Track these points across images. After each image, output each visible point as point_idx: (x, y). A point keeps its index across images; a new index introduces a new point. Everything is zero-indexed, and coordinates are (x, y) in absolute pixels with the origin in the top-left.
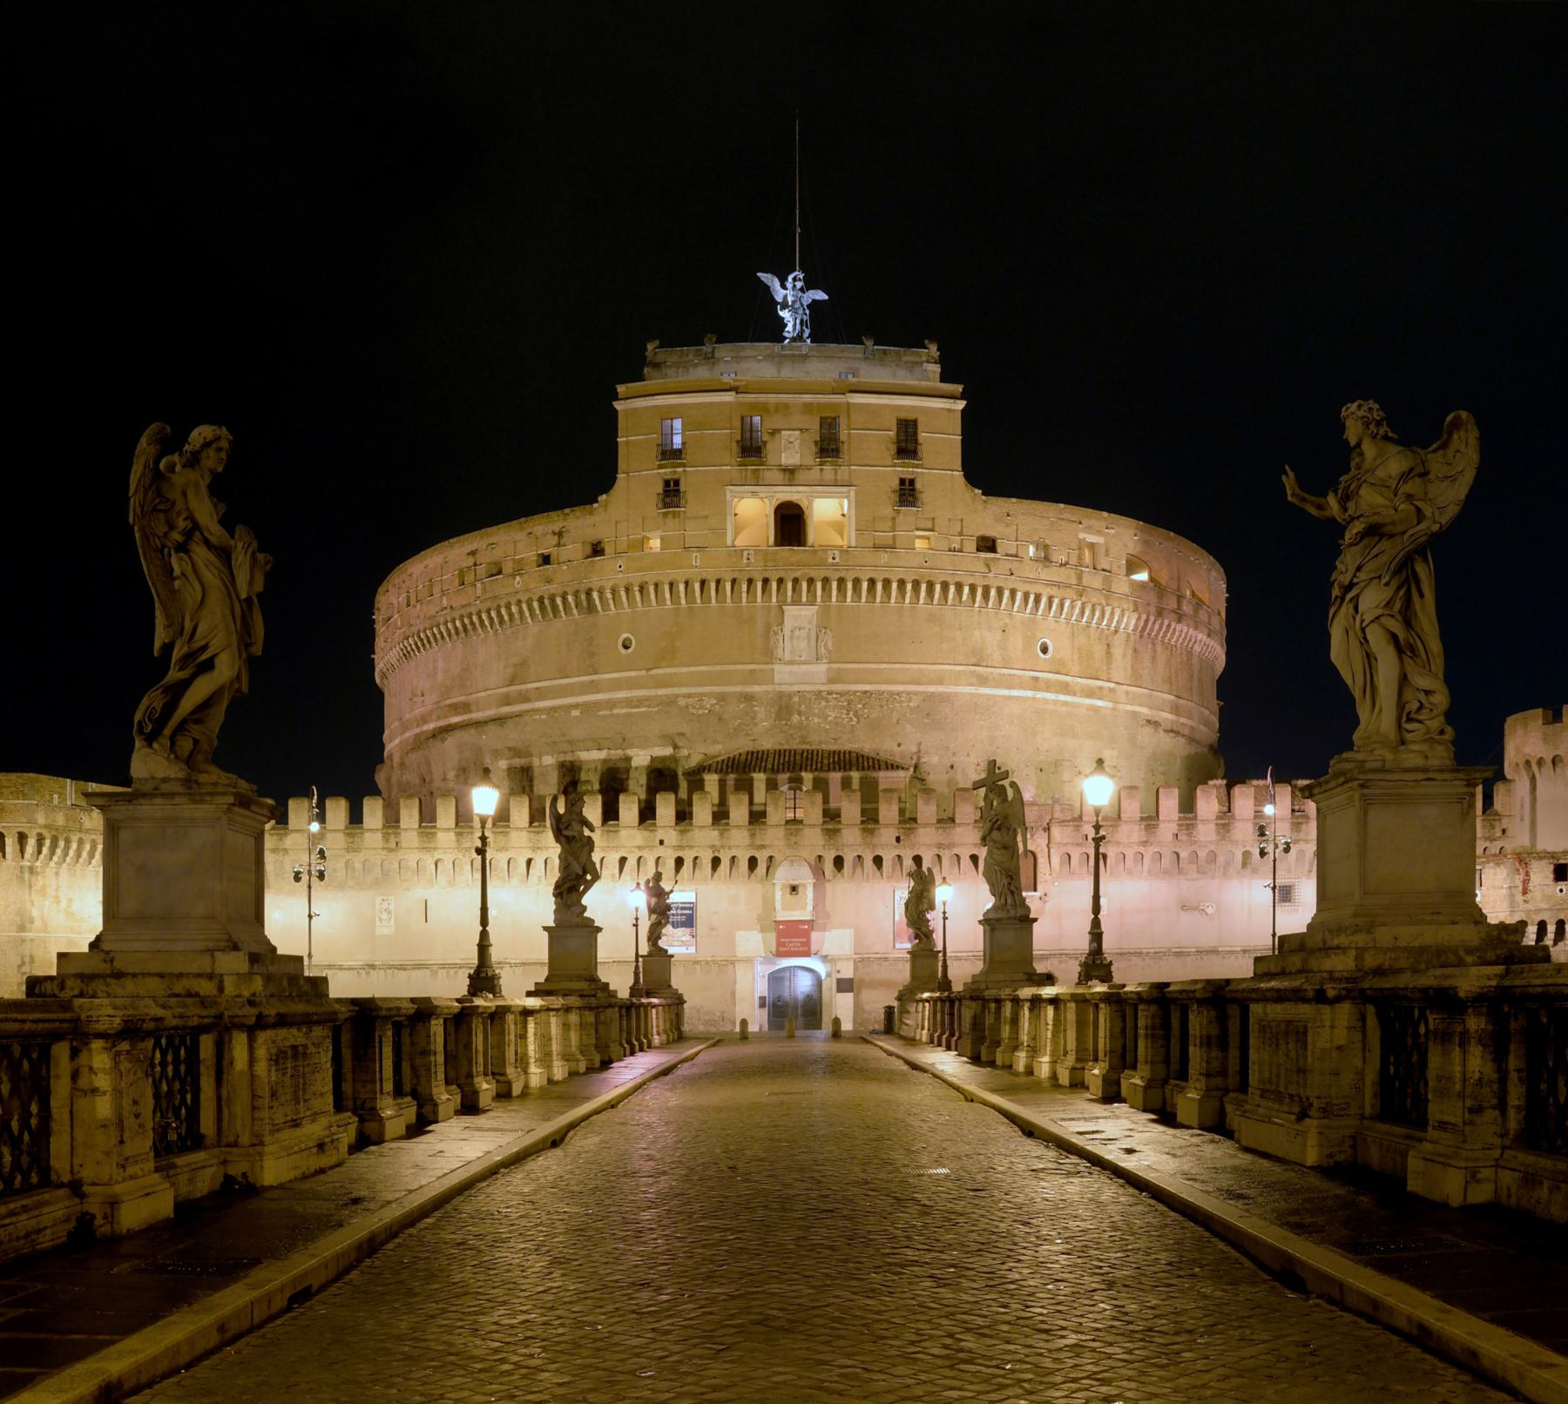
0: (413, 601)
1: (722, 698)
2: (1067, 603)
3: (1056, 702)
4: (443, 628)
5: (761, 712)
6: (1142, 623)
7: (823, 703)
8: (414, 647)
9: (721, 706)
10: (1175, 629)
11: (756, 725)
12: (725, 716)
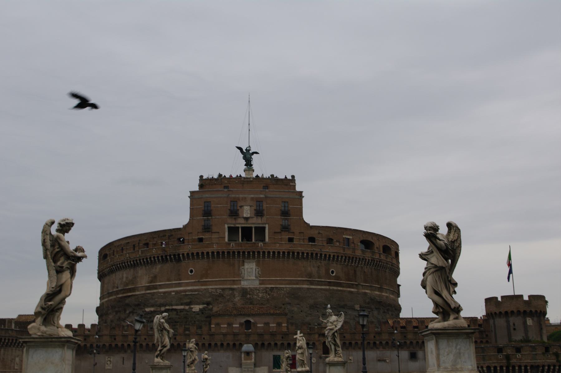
0: (115, 253)
1: (223, 289)
2: (340, 257)
3: (337, 290)
4: (126, 264)
5: (236, 294)
6: (367, 263)
7: (258, 291)
8: (115, 269)
9: (223, 292)
10: (379, 264)
11: (235, 298)
12: (225, 295)
